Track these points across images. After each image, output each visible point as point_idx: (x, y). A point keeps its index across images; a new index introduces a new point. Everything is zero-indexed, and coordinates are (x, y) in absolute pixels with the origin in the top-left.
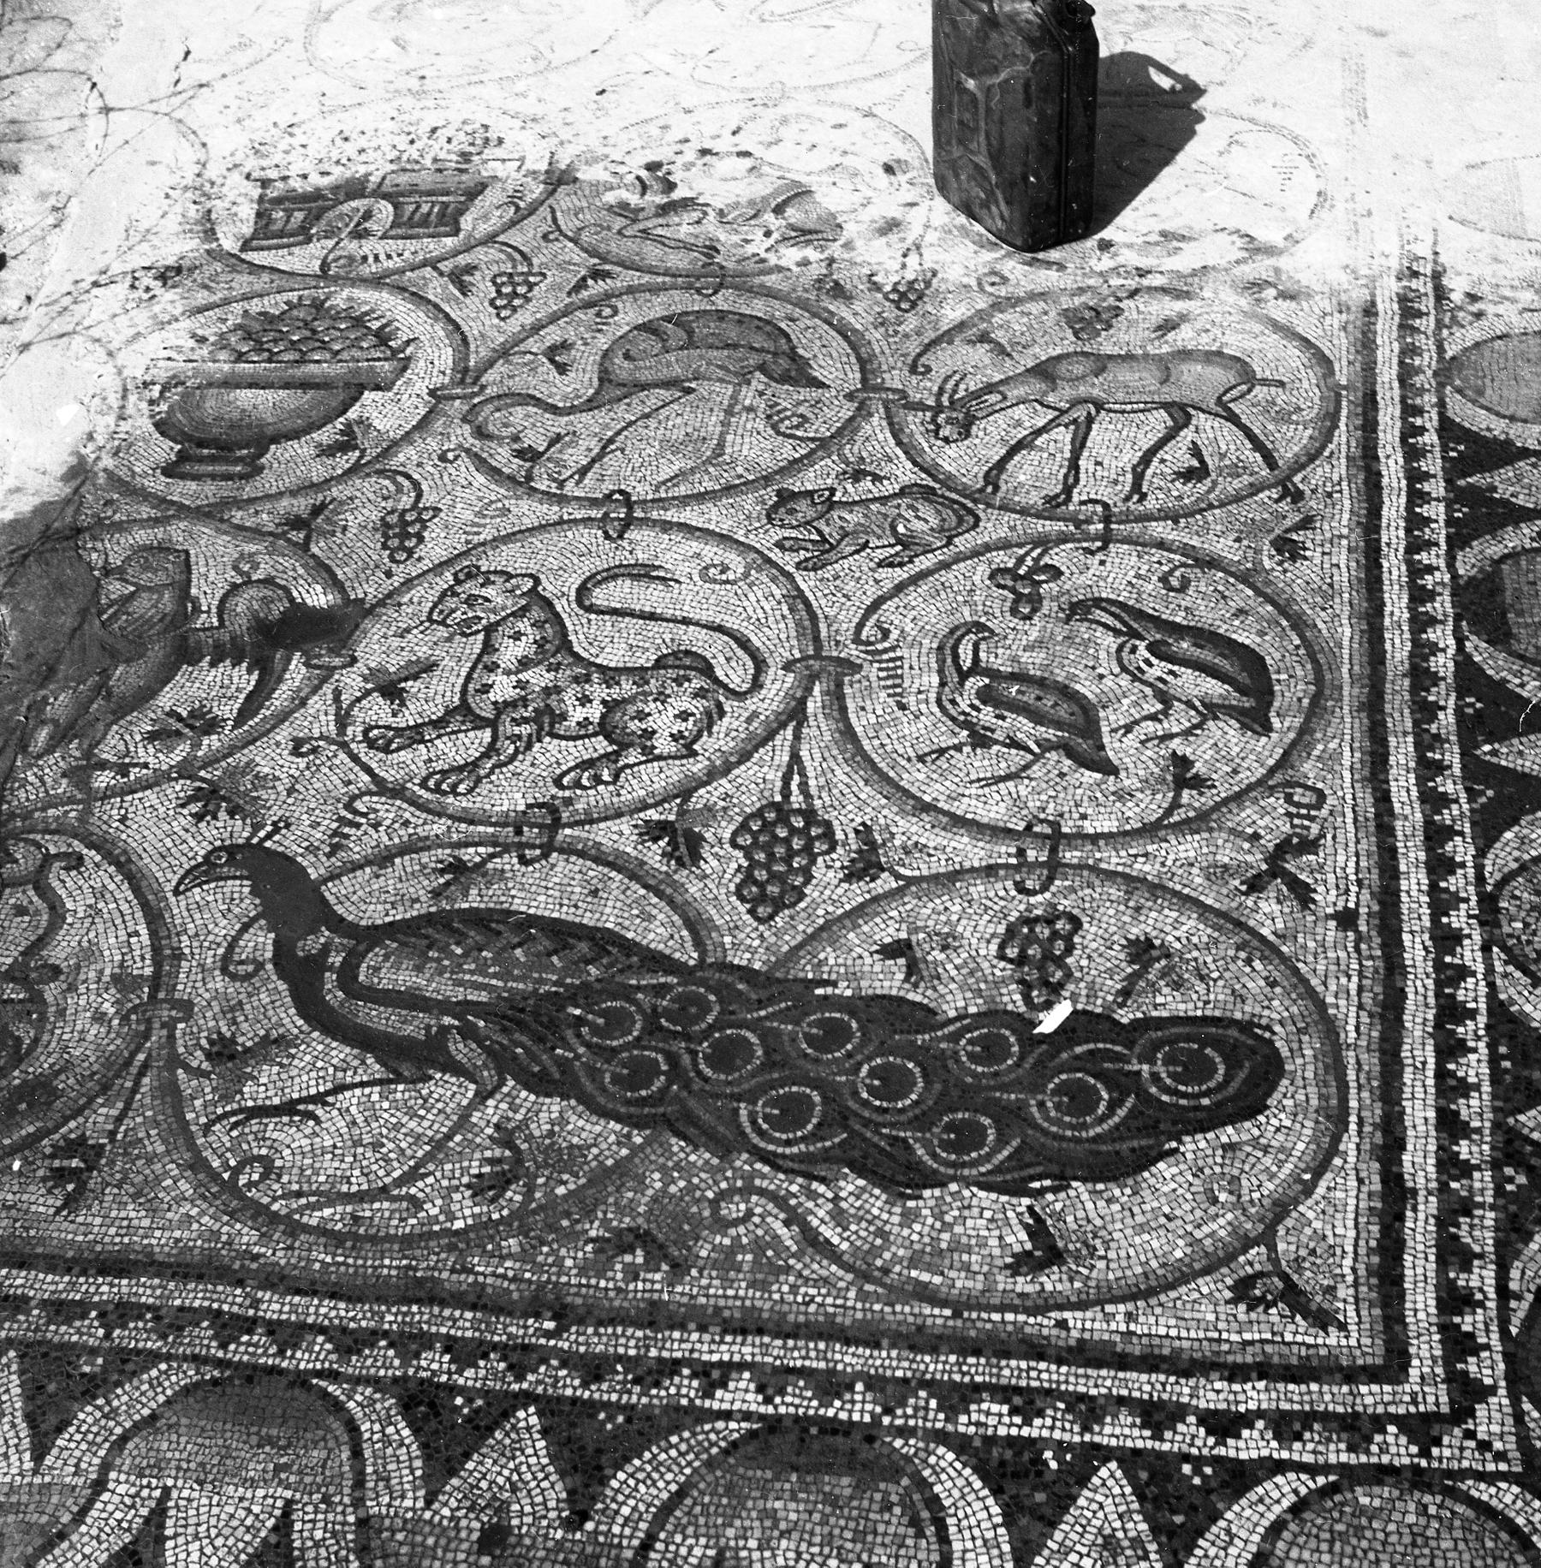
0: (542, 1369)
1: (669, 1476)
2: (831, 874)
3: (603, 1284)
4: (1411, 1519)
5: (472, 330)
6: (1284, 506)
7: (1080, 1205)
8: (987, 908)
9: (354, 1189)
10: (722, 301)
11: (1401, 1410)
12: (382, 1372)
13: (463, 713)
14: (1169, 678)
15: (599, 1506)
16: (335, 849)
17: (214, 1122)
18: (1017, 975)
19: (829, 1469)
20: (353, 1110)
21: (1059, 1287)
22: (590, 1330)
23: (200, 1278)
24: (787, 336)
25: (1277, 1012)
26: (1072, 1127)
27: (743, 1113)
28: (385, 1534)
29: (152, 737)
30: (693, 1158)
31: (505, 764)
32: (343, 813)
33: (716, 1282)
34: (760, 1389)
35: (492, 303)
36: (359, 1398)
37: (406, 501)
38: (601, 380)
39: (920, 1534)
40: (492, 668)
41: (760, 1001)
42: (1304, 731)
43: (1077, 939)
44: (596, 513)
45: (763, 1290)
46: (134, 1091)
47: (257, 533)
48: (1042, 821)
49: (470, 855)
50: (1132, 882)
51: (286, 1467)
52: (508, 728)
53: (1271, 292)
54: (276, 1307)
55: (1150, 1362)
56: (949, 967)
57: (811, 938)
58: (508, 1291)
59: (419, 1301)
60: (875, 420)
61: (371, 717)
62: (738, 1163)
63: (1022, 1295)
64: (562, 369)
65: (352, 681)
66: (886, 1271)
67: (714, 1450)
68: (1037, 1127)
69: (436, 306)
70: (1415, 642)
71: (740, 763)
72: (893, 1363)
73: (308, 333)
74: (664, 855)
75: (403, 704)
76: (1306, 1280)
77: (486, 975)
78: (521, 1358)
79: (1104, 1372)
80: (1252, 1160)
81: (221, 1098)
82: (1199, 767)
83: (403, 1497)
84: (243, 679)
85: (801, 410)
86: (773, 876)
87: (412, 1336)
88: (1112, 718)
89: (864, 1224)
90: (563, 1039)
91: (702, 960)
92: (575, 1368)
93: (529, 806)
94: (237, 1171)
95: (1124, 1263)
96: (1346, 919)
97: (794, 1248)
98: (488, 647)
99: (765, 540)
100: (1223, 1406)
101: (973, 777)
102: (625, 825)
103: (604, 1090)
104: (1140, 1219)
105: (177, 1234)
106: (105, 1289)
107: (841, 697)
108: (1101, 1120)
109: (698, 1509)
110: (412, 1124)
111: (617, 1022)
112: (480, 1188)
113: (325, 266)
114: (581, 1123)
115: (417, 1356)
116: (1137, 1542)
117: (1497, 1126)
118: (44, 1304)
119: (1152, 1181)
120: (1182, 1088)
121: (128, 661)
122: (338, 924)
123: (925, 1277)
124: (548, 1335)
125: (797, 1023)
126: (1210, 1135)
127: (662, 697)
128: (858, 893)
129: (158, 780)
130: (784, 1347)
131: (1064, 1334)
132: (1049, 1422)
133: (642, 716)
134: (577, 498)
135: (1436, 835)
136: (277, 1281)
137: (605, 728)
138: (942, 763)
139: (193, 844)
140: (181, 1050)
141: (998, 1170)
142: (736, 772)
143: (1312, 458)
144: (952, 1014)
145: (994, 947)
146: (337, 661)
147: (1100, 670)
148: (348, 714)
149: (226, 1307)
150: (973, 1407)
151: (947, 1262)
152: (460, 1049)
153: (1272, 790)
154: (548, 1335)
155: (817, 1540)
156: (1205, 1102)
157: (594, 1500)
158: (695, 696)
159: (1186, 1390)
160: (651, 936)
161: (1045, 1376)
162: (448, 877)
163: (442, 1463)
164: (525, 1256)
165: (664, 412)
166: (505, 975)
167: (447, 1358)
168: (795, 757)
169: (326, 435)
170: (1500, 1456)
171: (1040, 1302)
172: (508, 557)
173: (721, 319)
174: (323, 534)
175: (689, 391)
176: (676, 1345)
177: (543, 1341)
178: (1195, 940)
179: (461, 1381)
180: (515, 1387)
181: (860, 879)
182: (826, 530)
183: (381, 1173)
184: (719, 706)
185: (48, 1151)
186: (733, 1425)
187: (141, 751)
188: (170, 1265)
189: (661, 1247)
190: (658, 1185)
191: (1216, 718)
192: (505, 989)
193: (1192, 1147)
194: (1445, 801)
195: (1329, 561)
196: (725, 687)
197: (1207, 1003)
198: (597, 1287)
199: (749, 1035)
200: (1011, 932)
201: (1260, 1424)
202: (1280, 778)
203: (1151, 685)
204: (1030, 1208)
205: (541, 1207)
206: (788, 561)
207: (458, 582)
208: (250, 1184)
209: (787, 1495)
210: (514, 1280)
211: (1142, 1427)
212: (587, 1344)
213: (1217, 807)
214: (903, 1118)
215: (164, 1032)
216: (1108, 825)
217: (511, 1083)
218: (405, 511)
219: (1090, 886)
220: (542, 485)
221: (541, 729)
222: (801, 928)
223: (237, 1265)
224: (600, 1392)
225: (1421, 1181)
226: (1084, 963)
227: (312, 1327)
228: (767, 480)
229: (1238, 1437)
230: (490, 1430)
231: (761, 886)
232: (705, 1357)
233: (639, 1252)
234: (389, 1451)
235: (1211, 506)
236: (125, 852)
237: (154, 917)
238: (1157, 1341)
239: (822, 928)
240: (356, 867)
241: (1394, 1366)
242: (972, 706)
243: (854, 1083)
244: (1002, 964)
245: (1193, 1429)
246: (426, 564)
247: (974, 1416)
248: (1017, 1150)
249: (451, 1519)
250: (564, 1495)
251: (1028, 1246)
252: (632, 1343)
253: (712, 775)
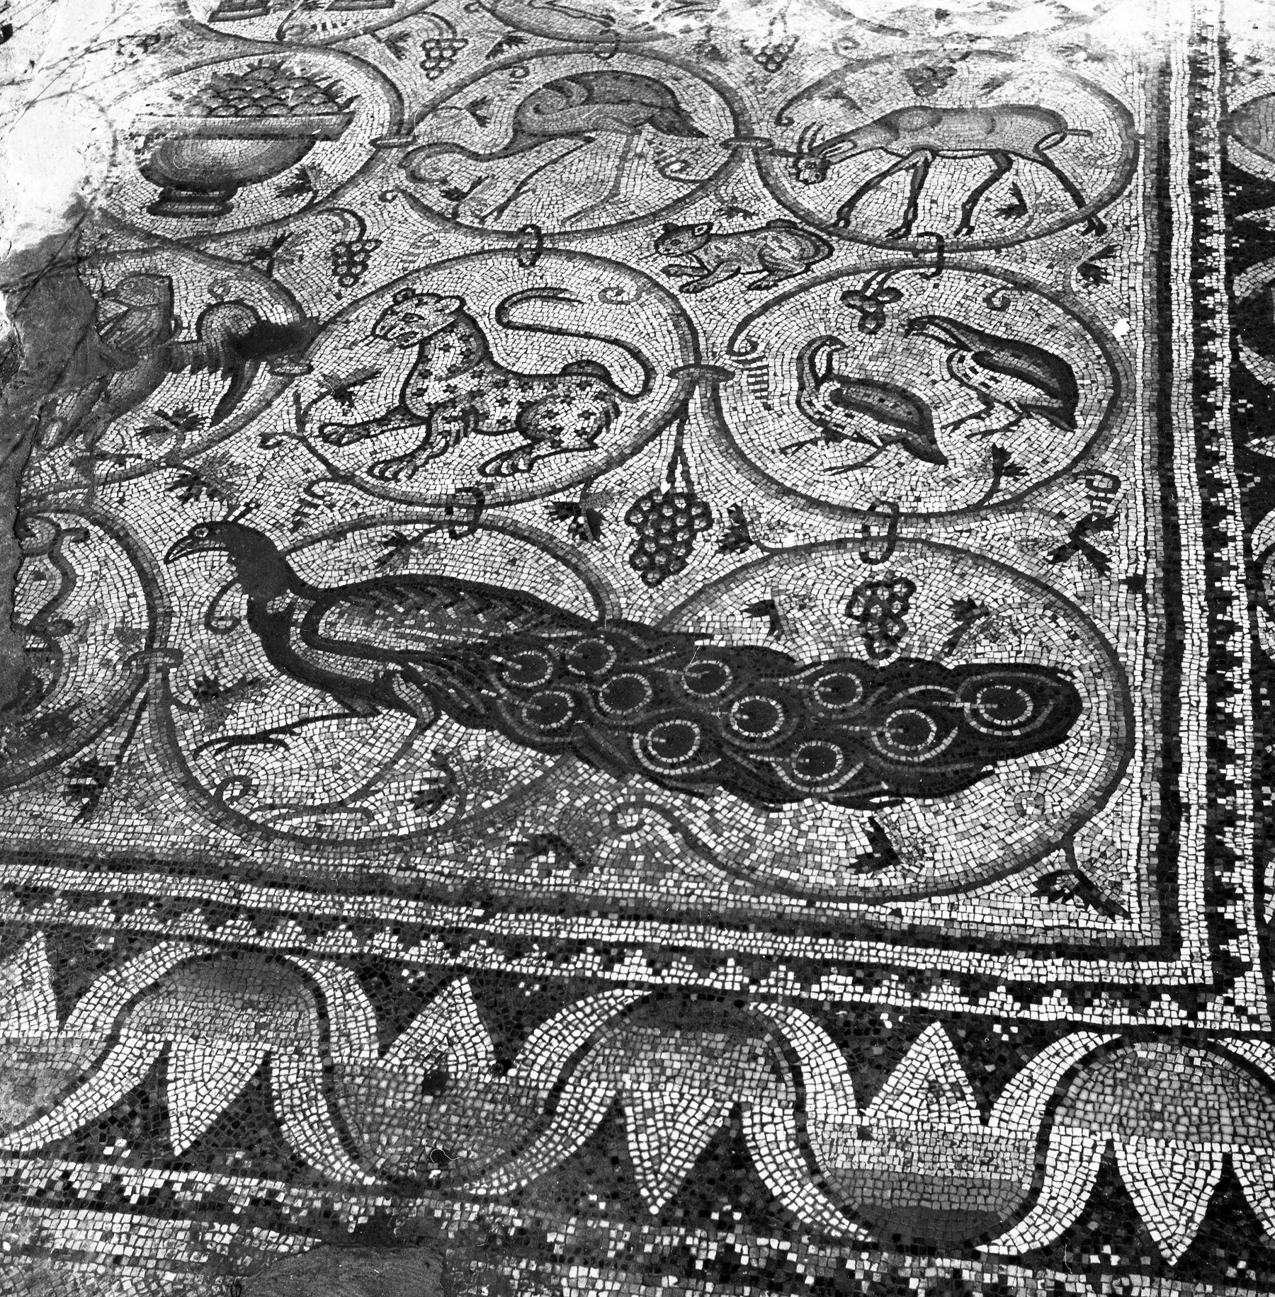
0: (473, 948)
1: (577, 1033)
2: (708, 546)
3: (522, 879)
4: (1179, 1069)
5: (405, 90)
6: (1089, 238)
7: (912, 817)
8: (837, 575)
9: (317, 802)
10: (618, 63)
11: (1174, 982)
12: (342, 950)
13: (402, 413)
14: (991, 383)
15: (520, 1057)
16: (297, 526)
17: (200, 749)
18: (862, 630)
19: (706, 1027)
20: (316, 739)
21: (894, 882)
22: (512, 917)
23: (192, 873)
24: (672, 93)
25: (1078, 661)
26: (907, 754)
27: (636, 742)
28: (347, 1079)
29: (144, 432)
30: (595, 778)
31: (437, 456)
32: (304, 496)
33: (614, 878)
34: (650, 964)
35: (422, 65)
36: (323, 970)
37: (352, 235)
38: (515, 131)
39: (780, 1079)
40: (426, 375)
41: (649, 651)
42: (1103, 427)
43: (911, 600)
44: (512, 244)
45: (653, 885)
46: (136, 722)
47: (228, 262)
48: (883, 503)
49: (409, 530)
50: (958, 554)
51: (266, 1026)
52: (440, 425)
53: (1081, 55)
54: (255, 897)
55: (969, 943)
56: (806, 623)
57: (691, 599)
58: (444, 886)
59: (372, 893)
60: (746, 165)
61: (325, 417)
62: (632, 783)
63: (864, 889)
64: (482, 121)
65: (309, 387)
66: (753, 869)
67: (613, 1013)
68: (877, 753)
69: (375, 68)
70: (1198, 353)
71: (633, 454)
72: (759, 943)
73: (267, 92)
74: (570, 531)
75: (352, 405)
76: (1097, 876)
77: (422, 628)
78: (455, 939)
79: (930, 951)
80: (1054, 780)
81: (208, 728)
82: (1015, 458)
83: (361, 1049)
84: (219, 385)
85: (684, 156)
86: (661, 549)
87: (366, 921)
88: (943, 417)
89: (735, 832)
90: (488, 681)
91: (601, 618)
92: (500, 946)
93: (458, 490)
94: (221, 788)
95: (948, 863)
96: (1136, 584)
97: (678, 851)
98: (423, 358)
99: (653, 268)
100: (1027, 978)
101: (827, 466)
102: (538, 506)
103: (522, 723)
104: (961, 828)
105: (173, 838)
106: (116, 883)
107: (716, 399)
108: (929, 749)
109: (600, 1059)
110: (364, 750)
111: (531, 668)
112: (420, 802)
113: (280, 34)
114: (503, 750)
115: (371, 937)
116: (956, 1086)
117: (1257, 753)
118: (64, 894)
119: (972, 797)
120: (998, 722)
121: (122, 369)
122: (301, 588)
123: (785, 874)
124: (478, 920)
125: (680, 669)
126: (1020, 760)
127: (568, 400)
128: (731, 562)
129: (152, 467)
130: (670, 930)
131: (898, 920)
132: (885, 990)
133: (551, 415)
134: (496, 232)
135: (1212, 514)
136: (255, 876)
137: (521, 426)
138: (800, 453)
139: (180, 521)
140: (174, 690)
141: (845, 788)
142: (630, 462)
143: (1114, 197)
144: (808, 661)
145: (843, 606)
146: (297, 370)
147: (933, 377)
148: (306, 413)
149: (214, 897)
150: (824, 978)
151: (803, 862)
152: (403, 691)
153: (1076, 477)
154: (478, 920)
155: (697, 1084)
156: (1017, 733)
157: (516, 1051)
158: (596, 398)
159: (998, 966)
160: (560, 597)
161: (882, 954)
162: (391, 548)
163: (392, 1023)
164: (457, 857)
165: (568, 159)
166: (440, 630)
167: (395, 938)
168: (679, 450)
169: (284, 179)
170: (1254, 1019)
171: (879, 894)
172: (438, 282)
173: (617, 78)
174: (283, 262)
175: (589, 140)
176: (581, 929)
177: (473, 925)
178: (1009, 601)
179: (407, 957)
180: (451, 962)
181: (732, 550)
182: (705, 258)
183: (340, 790)
184: (616, 406)
185: (66, 771)
186: (628, 992)
187: (135, 444)
188: (167, 863)
189: (569, 849)
190: (567, 800)
191: (1029, 417)
192: (439, 641)
193: (1005, 769)
194: (1220, 486)
195: (1128, 282)
196: (621, 391)
197: (1019, 652)
198: (517, 882)
199: (640, 678)
200: (856, 592)
201: (1058, 993)
202: (1082, 467)
203: (975, 389)
204: (871, 819)
205: (471, 818)
206: (673, 285)
207: (397, 303)
208: (232, 799)
209: (672, 1048)
210: (449, 876)
211: (961, 994)
212: (510, 928)
213: (1029, 491)
214: (767, 746)
215: (159, 675)
216: (938, 506)
217: (445, 717)
218: (351, 243)
219: (923, 556)
220: (466, 221)
221: (467, 426)
222: (683, 591)
223: (222, 864)
224: (522, 966)
225: (1193, 797)
226: (917, 619)
227: (284, 913)
228: (655, 215)
229: (1040, 1003)
230: (431, 996)
231: (651, 556)
232: (606, 938)
233: (551, 854)
234: (349, 1013)
235: (1028, 238)
236: (123, 528)
237: (149, 581)
238: (974, 927)
239: (701, 591)
240: (315, 540)
241: (1169, 946)
242: (826, 407)
243: (727, 717)
244: (849, 621)
245: (1003, 997)
246: (369, 288)
247: (824, 986)
248: (860, 773)
249: (400, 1067)
250: (491, 1048)
251: (869, 849)
252: (546, 927)
253: (610, 464)
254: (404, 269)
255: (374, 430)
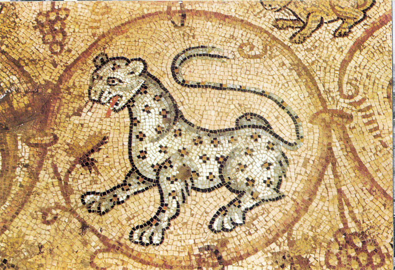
40: (141, 137)
71: (311, 200)
127: (249, 152)
133: (242, 167)
148: (66, 184)
168: (340, 191)
182: (297, 12)
196: (282, 140)
207: (98, 68)
254: (94, 35)
255: (122, 195)
